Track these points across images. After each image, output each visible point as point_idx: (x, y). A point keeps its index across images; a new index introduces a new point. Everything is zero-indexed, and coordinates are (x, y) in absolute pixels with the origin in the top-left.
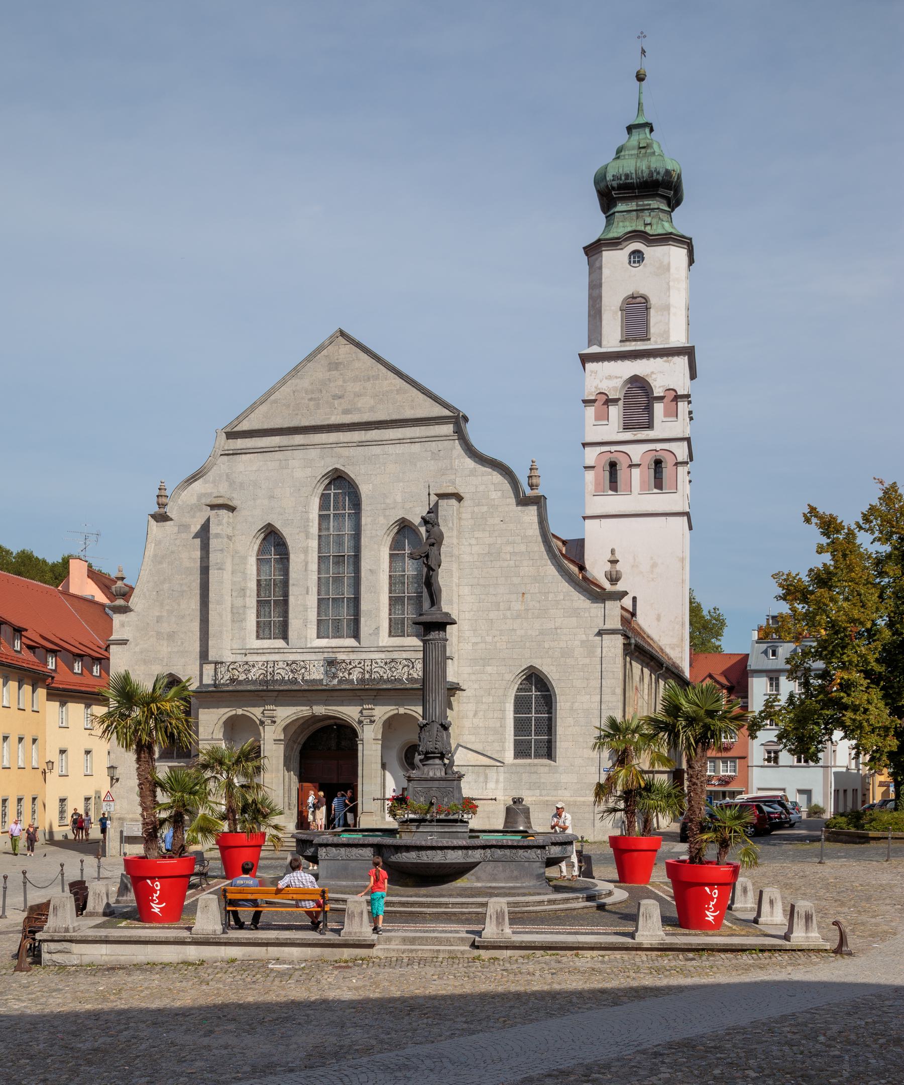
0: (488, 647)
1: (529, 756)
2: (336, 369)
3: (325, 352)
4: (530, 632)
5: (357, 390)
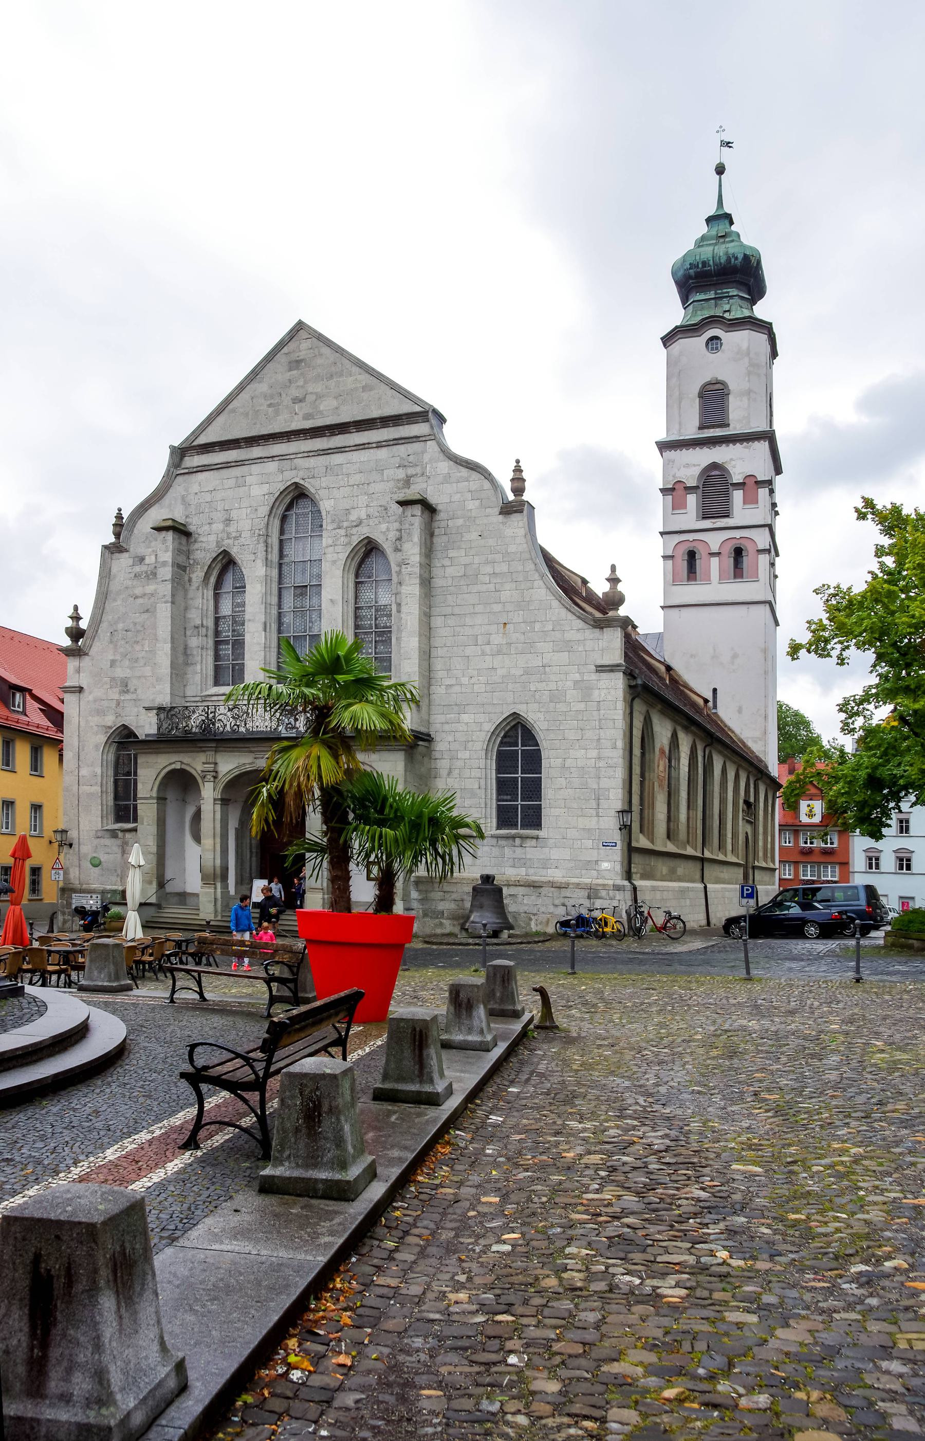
0: (464, 690)
1: (515, 826)
2: (297, 368)
3: (285, 350)
4: (513, 671)
5: (319, 390)
